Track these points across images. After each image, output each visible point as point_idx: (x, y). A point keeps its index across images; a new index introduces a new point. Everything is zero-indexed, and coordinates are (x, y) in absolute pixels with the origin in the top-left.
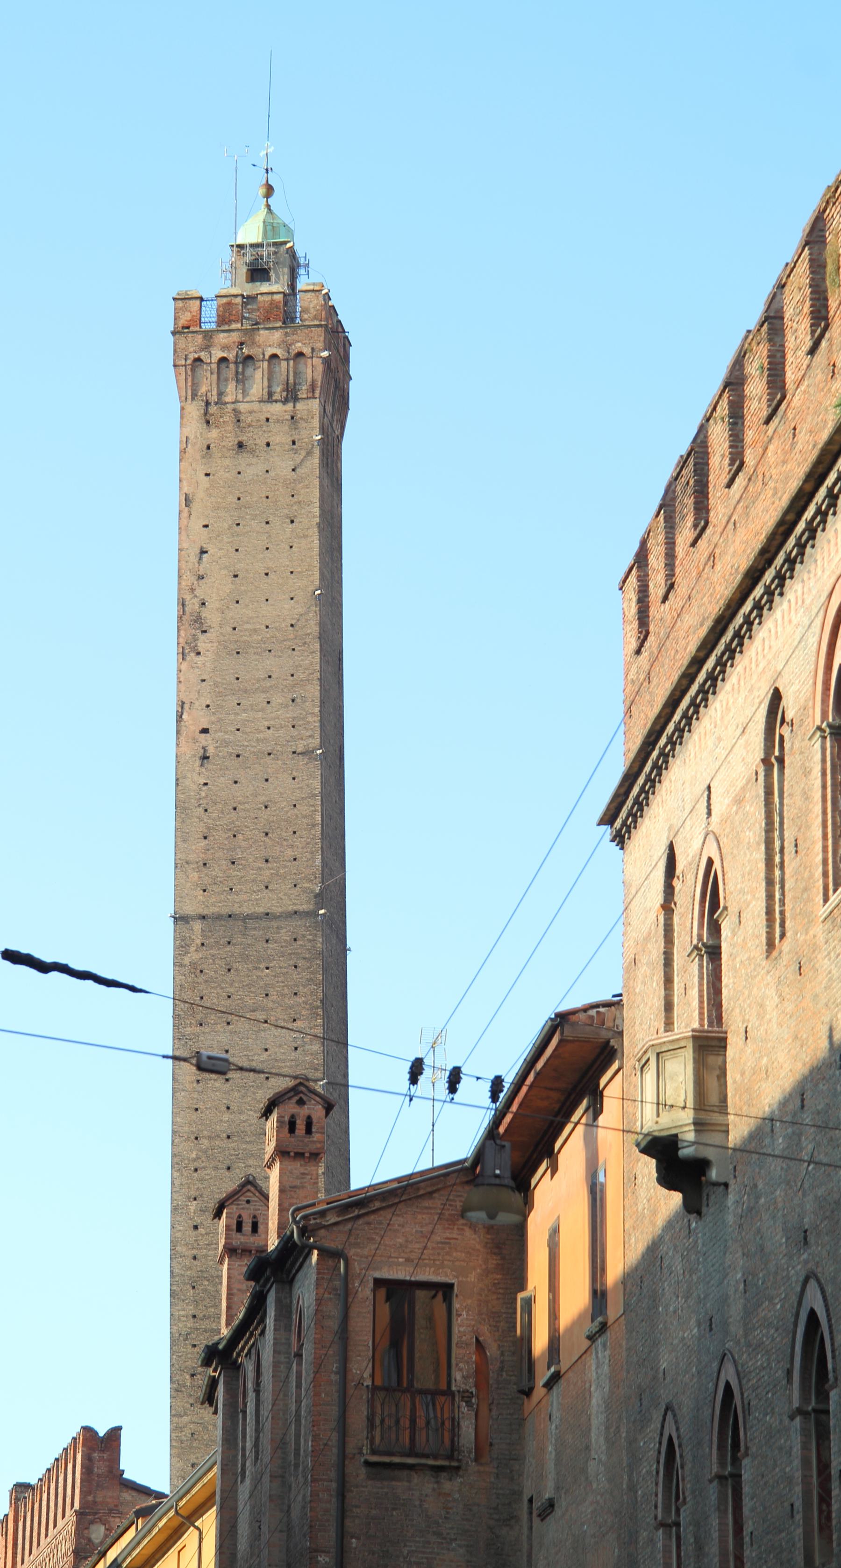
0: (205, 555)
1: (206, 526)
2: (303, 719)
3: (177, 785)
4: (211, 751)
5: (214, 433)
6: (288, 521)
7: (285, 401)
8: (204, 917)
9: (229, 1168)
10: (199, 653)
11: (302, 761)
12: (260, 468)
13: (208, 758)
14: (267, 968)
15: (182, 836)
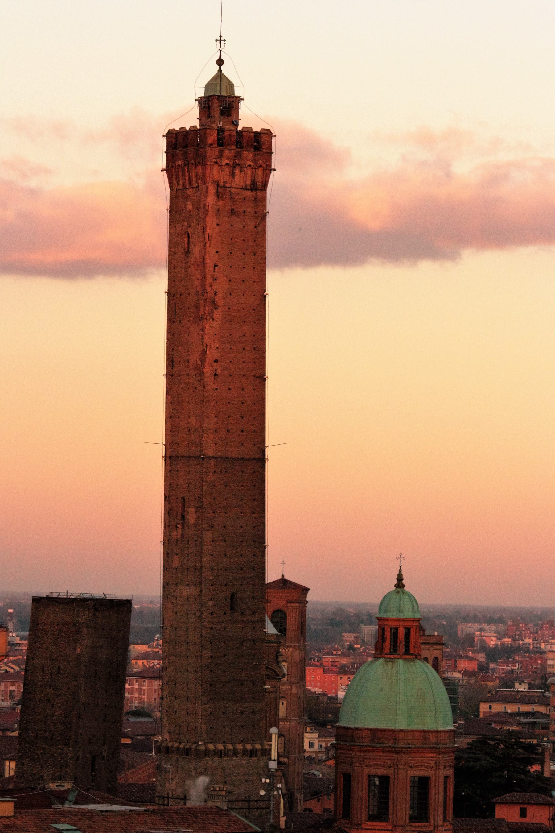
0: (216, 268)
1: (217, 252)
2: (258, 359)
4: (219, 371)
5: (221, 203)
6: (253, 254)
7: (252, 190)
10: (213, 320)
13: (217, 375)
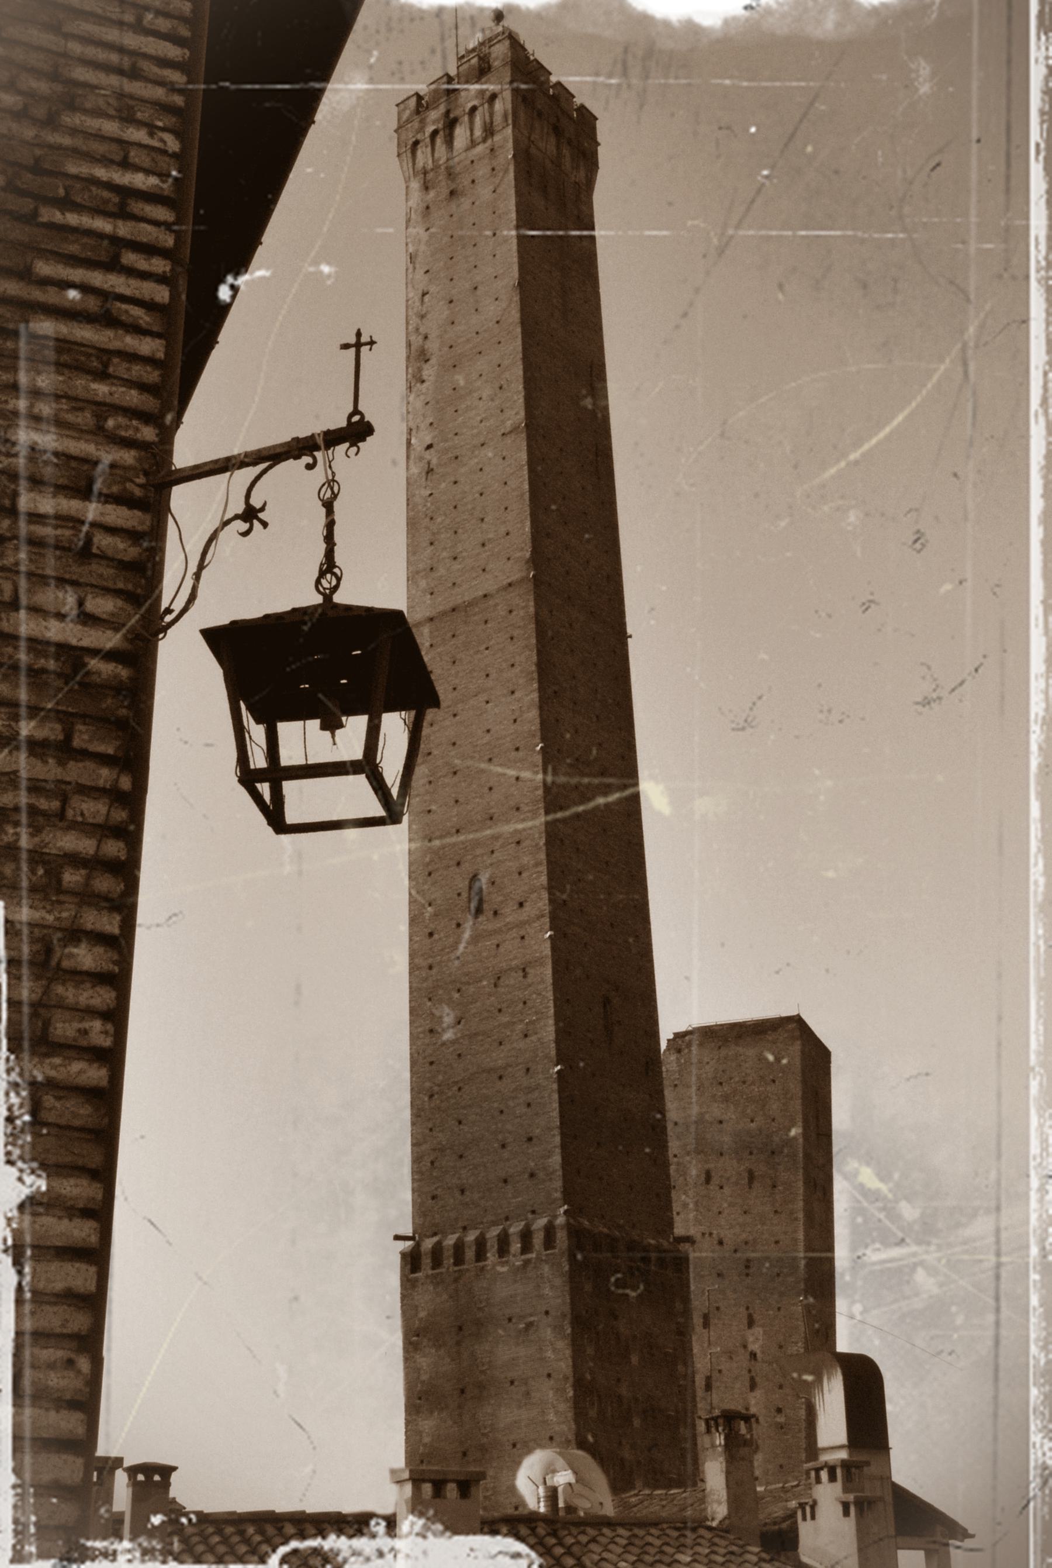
1: (427, 271)
3: (408, 505)
5: (432, 193)
8: (431, 619)
9: (458, 864)
11: (508, 440)
12: (469, 202)
14: (487, 649)
15: (413, 550)
